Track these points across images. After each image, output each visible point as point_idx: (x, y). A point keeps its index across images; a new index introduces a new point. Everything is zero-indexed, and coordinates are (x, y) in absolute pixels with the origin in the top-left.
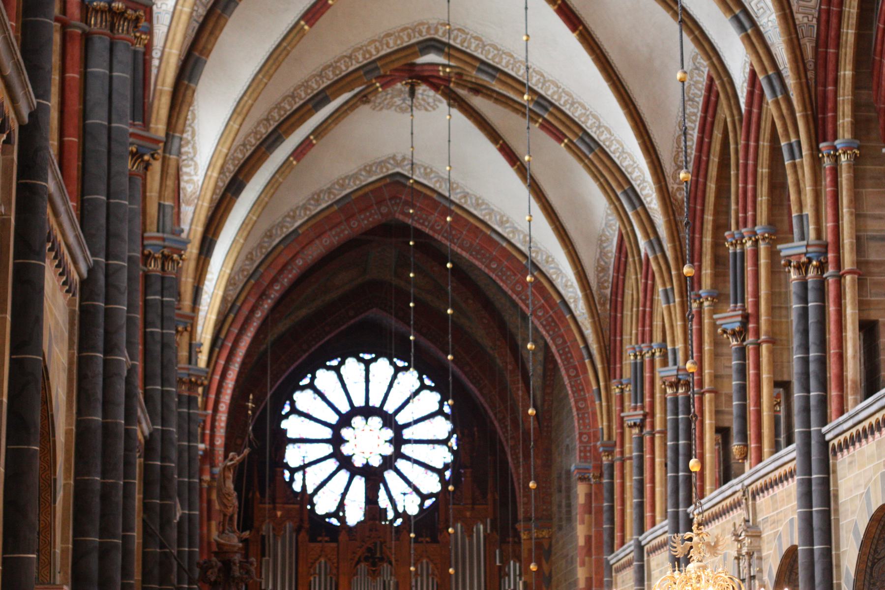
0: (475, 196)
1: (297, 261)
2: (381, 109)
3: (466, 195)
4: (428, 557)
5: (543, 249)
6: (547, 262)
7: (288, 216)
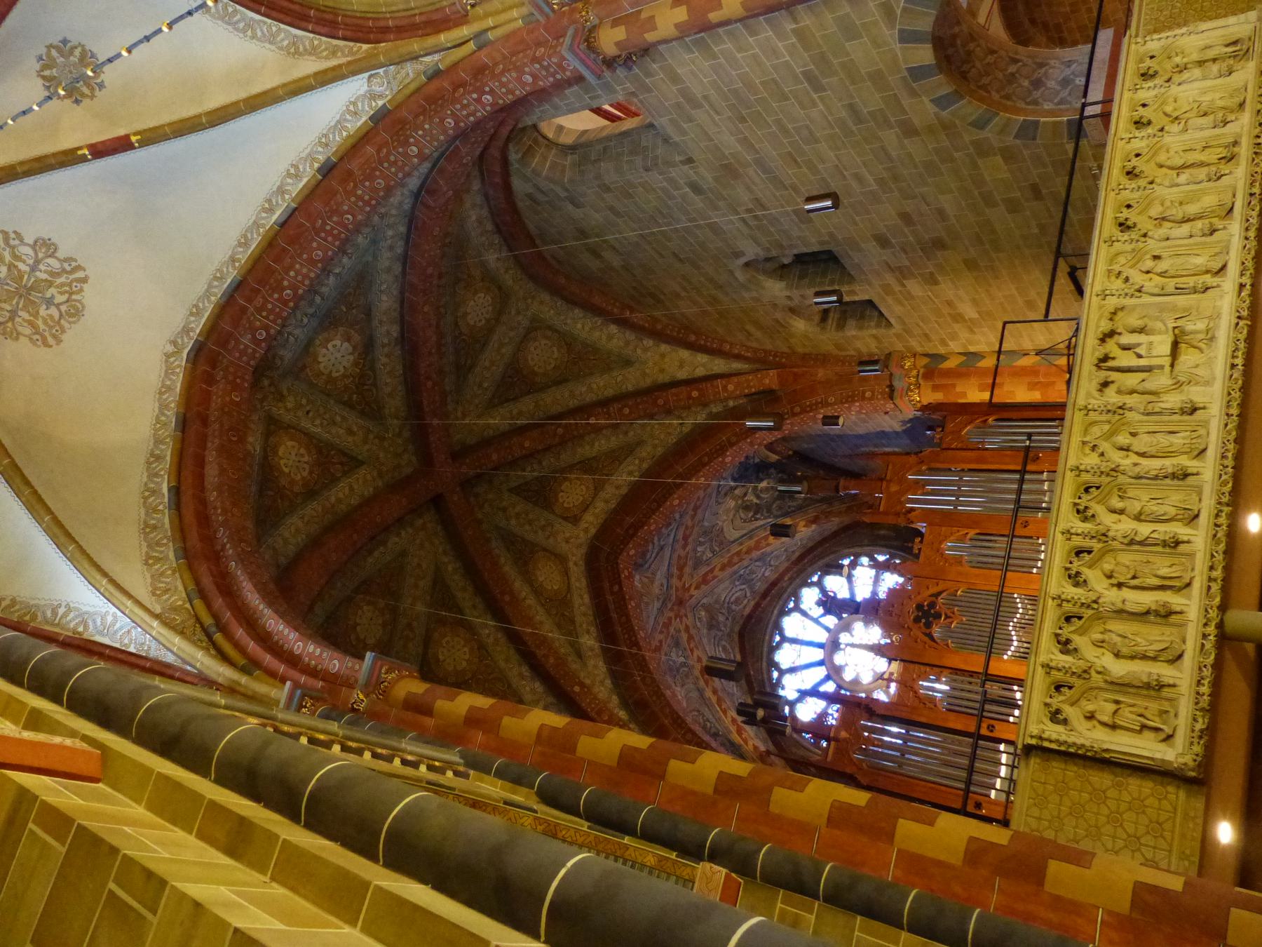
0: (236, 247)
1: (212, 499)
2: (59, 341)
3: (233, 260)
4: (941, 543)
5: (307, 151)
6: (327, 145)
7: (146, 498)
